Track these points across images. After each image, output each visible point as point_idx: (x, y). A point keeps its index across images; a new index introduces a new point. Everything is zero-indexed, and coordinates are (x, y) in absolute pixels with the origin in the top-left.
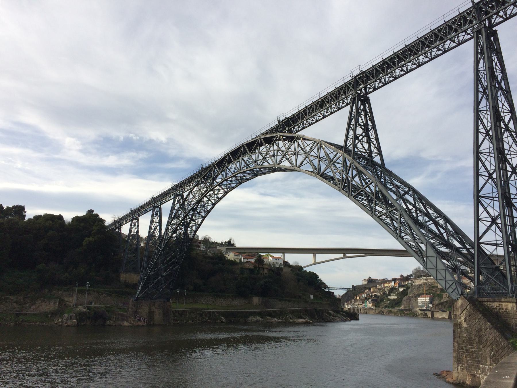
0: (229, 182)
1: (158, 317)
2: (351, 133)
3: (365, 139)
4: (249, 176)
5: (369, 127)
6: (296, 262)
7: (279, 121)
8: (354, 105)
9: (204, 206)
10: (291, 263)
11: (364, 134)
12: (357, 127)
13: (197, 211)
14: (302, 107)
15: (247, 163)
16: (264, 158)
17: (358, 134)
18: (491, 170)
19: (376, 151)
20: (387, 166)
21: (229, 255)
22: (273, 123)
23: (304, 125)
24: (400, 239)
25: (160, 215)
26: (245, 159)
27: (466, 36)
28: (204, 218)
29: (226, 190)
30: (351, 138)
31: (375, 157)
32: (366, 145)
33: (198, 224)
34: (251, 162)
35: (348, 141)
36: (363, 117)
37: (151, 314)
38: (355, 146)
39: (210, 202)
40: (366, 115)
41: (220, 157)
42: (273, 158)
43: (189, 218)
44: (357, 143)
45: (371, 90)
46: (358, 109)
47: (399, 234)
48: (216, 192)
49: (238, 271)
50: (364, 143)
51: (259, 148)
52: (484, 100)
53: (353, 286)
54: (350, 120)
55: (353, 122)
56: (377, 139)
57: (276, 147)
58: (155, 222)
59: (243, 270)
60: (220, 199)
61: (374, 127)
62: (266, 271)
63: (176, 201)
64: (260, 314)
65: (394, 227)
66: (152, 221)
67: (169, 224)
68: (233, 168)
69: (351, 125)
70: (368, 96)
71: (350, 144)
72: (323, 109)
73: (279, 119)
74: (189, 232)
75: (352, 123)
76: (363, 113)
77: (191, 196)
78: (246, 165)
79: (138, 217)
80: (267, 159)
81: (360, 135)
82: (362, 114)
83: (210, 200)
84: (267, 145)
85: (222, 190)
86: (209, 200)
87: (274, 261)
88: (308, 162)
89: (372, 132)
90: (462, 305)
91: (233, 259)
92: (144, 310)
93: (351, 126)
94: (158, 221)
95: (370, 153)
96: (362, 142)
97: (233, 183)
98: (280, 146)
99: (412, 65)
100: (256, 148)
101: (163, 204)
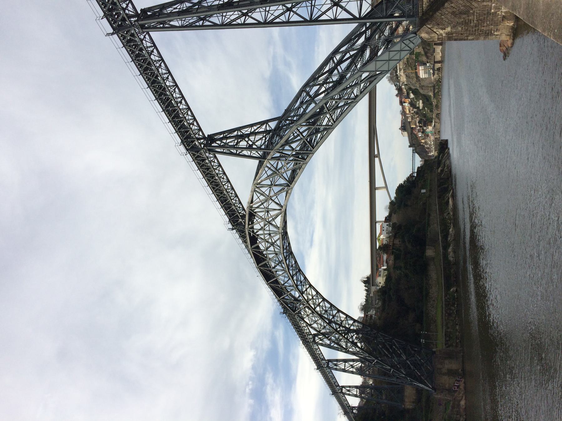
0: (299, 283)
1: (454, 365)
2: (245, 152)
3: (252, 138)
4: (292, 261)
5: (239, 134)
6: (386, 208)
7: (233, 229)
8: (216, 150)
9: (326, 311)
10: (387, 214)
11: (247, 139)
12: (239, 146)
13: (332, 319)
14: (218, 205)
15: (277, 263)
16: (272, 244)
17: (247, 145)
18: (283, 9)
19: (264, 127)
20: (280, 114)
21: (380, 283)
22: (235, 235)
23: (237, 202)
24: (358, 99)
25: (337, 360)
26: (273, 265)
27: (147, 40)
28: (339, 311)
29: (308, 286)
30: (251, 152)
31: (271, 127)
32: (258, 137)
33: (346, 318)
34: (277, 259)
35: (254, 155)
36: (228, 141)
37: (451, 373)
38: (259, 148)
39: (321, 304)
40: (226, 138)
41: (272, 293)
42: (272, 235)
43: (339, 328)
44: (256, 146)
45: (201, 134)
46: (220, 146)
47: (353, 100)
48: (310, 297)
49: (398, 272)
50: (255, 139)
51: (261, 250)
52: (212, 19)
53: (410, 146)
54: (231, 154)
56: (251, 126)
57: (260, 232)
58: (345, 367)
59: (396, 267)
60: (317, 292)
62: (397, 242)
63: (321, 342)
64: (445, 248)
65: (344, 105)
66: (344, 370)
67: (347, 352)
68: (283, 278)
69: (236, 153)
70: (206, 136)
71: (257, 154)
72: (220, 182)
73: (231, 229)
74: (355, 328)
75: (235, 151)
76: (224, 141)
77: (315, 326)
78: (280, 264)
79: (340, 386)
80: (273, 241)
81: (248, 143)
82: (225, 142)
83: (319, 304)
84: (258, 242)
85: (308, 290)
86: (319, 305)
87: (385, 232)
88: (277, 197)
89: (244, 131)
90: (427, 33)
91: (384, 279)
92: (446, 381)
93: (238, 152)
94: (344, 363)
96: (255, 141)
97: (299, 278)
98: (260, 227)
99: (176, 92)
100: (261, 253)
101: (324, 358)
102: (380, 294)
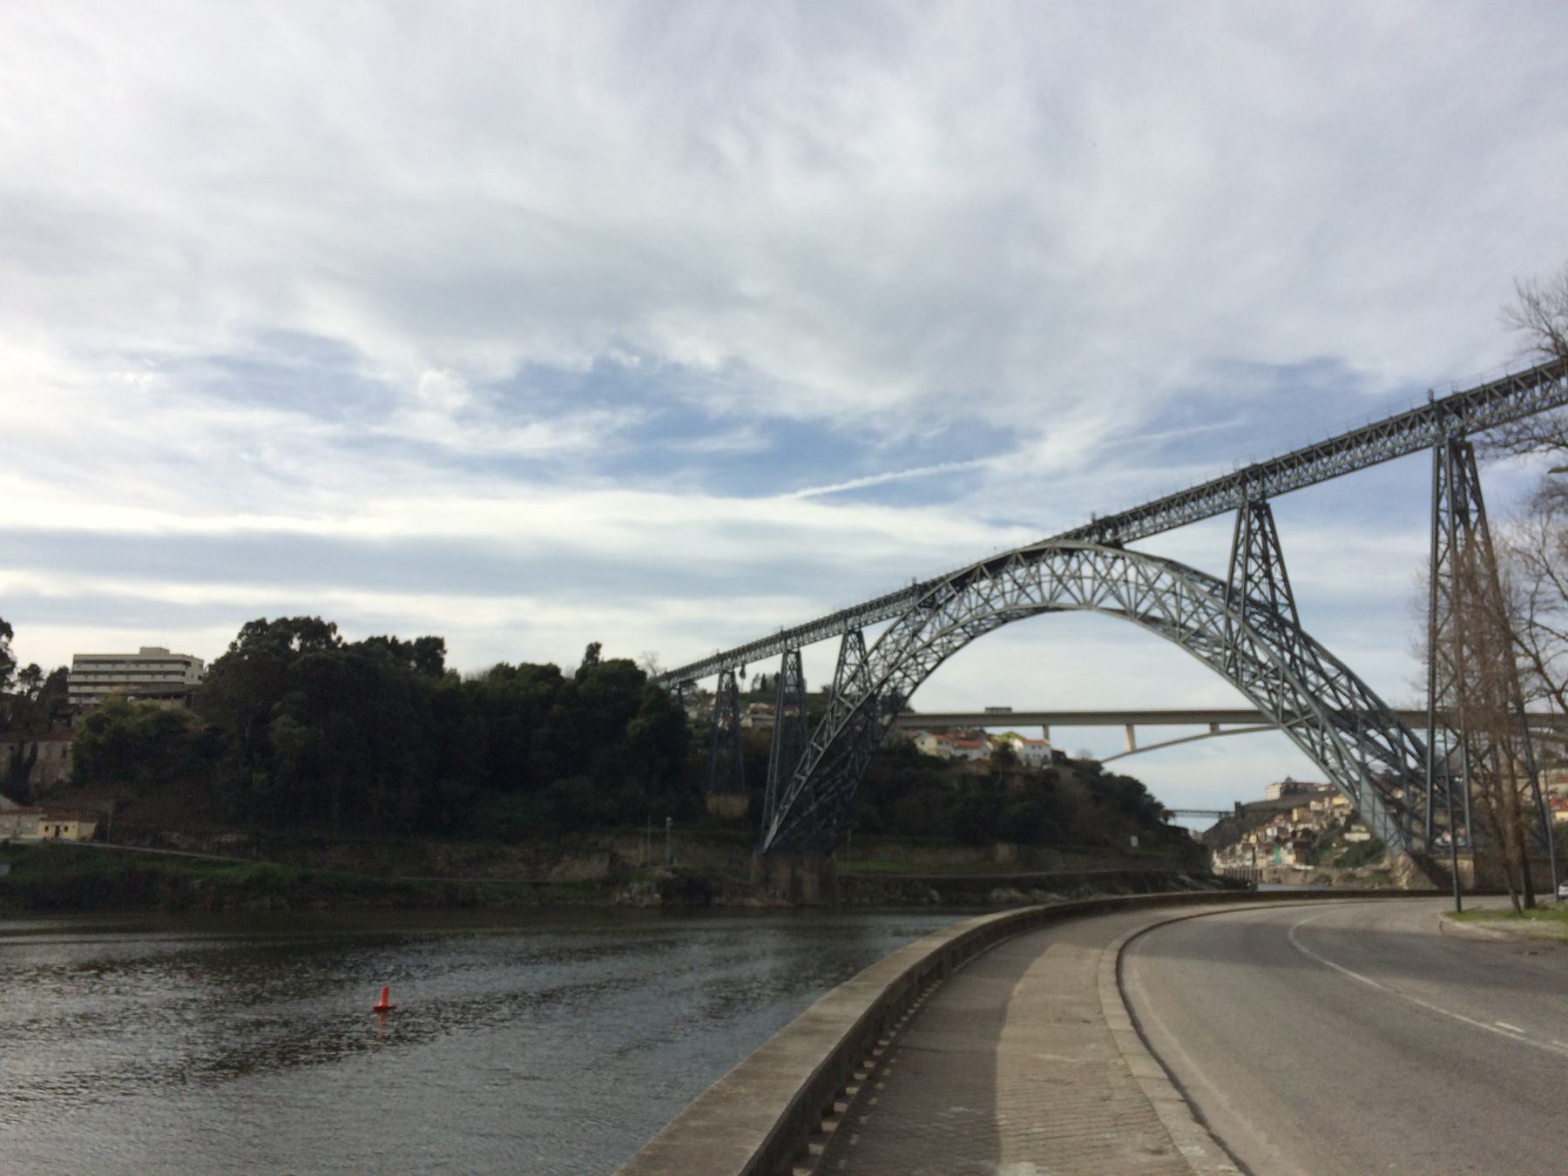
1: (809, 890)
6: (1084, 751)
10: (1071, 755)
20: (1306, 627)
21: (923, 743)
22: (1084, 521)
24: (1321, 764)
37: (796, 884)
40: (1264, 535)
47: (1320, 756)
49: (955, 784)
54: (1236, 547)
55: (1241, 550)
56: (1285, 580)
59: (965, 778)
61: (1280, 558)
62: (1017, 782)
64: (1017, 884)
65: (1312, 741)
87: (1029, 751)
90: (1403, 865)
91: (933, 753)
92: (782, 873)
95: (1274, 604)
102: (904, 743)
